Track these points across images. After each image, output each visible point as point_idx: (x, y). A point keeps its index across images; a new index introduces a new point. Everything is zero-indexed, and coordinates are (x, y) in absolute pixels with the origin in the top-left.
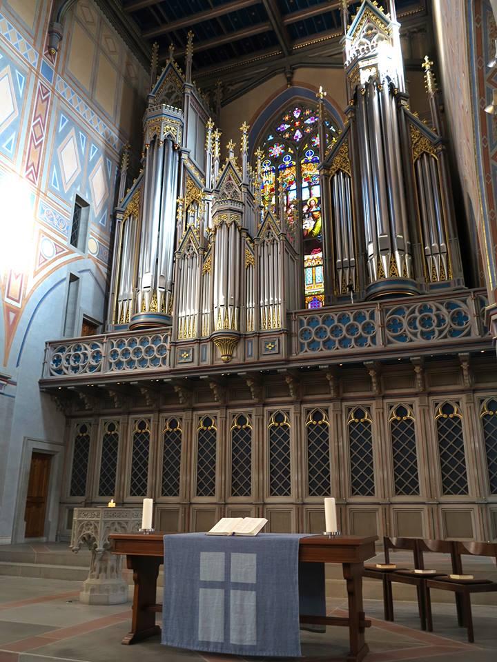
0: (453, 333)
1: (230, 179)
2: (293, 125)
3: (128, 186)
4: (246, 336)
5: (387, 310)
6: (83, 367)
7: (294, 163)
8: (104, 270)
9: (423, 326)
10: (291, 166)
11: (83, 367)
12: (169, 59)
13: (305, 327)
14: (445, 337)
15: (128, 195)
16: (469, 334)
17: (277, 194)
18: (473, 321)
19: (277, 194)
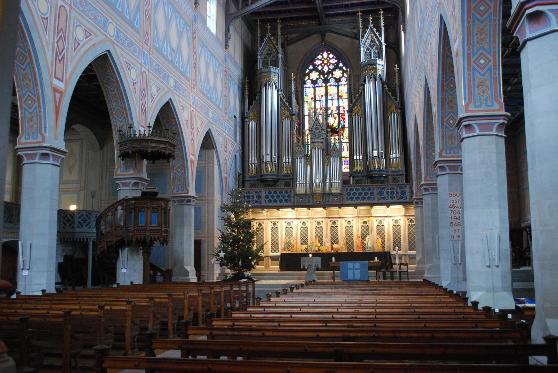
0: (401, 198)
1: (317, 125)
2: (323, 62)
3: (250, 104)
4: (326, 194)
5: (379, 188)
6: (252, 201)
7: (324, 85)
8: (241, 148)
9: (391, 194)
10: (322, 86)
11: (252, 201)
12: (268, 33)
13: (349, 191)
14: (398, 199)
15: (250, 109)
16: (406, 199)
17: (315, 101)
18: (408, 195)
19: (315, 101)
